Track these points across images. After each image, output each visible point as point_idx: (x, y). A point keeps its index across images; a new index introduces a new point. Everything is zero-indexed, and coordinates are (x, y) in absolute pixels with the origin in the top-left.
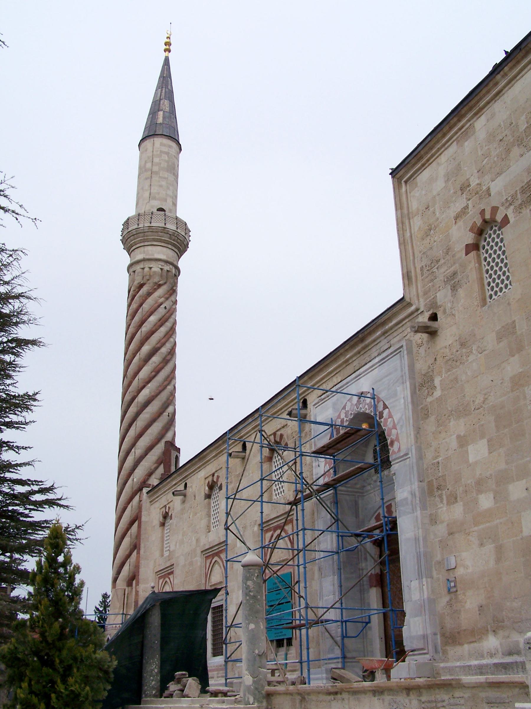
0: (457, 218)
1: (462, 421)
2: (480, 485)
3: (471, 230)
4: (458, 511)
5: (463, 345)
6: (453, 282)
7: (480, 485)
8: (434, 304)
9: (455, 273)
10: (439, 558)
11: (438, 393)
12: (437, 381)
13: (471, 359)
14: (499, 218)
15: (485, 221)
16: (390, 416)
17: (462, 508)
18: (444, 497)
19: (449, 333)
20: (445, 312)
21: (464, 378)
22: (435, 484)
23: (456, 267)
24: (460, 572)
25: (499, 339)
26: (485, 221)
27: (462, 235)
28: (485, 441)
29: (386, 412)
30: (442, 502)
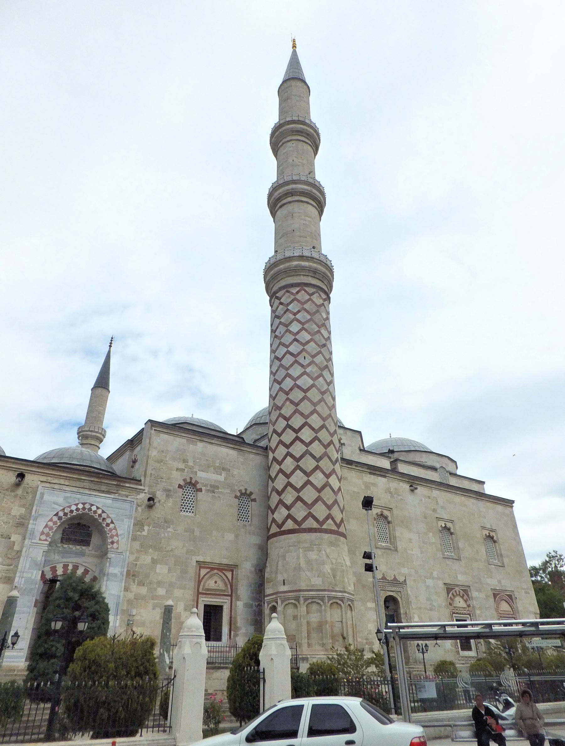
0: (177, 469)
1: (157, 553)
2: (160, 584)
3: (184, 480)
4: (143, 590)
5: (166, 522)
6: (168, 493)
7: (160, 584)
8: (154, 494)
9: (170, 490)
10: (125, 608)
11: (145, 533)
12: (146, 528)
13: (169, 529)
14: (198, 486)
15: (191, 482)
16: (115, 528)
17: (146, 590)
18: (136, 581)
19: (159, 512)
20: (159, 501)
21: (163, 535)
22: (132, 573)
23: (172, 488)
24: (137, 618)
25: (186, 531)
26: (191, 482)
27: (178, 478)
28: (167, 567)
29: (112, 526)
30: (134, 582)
